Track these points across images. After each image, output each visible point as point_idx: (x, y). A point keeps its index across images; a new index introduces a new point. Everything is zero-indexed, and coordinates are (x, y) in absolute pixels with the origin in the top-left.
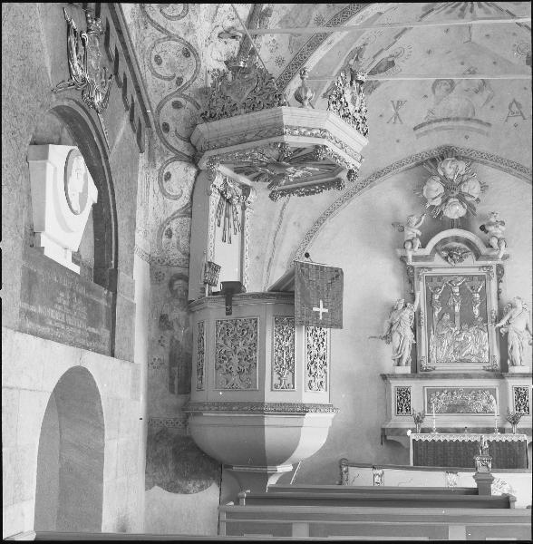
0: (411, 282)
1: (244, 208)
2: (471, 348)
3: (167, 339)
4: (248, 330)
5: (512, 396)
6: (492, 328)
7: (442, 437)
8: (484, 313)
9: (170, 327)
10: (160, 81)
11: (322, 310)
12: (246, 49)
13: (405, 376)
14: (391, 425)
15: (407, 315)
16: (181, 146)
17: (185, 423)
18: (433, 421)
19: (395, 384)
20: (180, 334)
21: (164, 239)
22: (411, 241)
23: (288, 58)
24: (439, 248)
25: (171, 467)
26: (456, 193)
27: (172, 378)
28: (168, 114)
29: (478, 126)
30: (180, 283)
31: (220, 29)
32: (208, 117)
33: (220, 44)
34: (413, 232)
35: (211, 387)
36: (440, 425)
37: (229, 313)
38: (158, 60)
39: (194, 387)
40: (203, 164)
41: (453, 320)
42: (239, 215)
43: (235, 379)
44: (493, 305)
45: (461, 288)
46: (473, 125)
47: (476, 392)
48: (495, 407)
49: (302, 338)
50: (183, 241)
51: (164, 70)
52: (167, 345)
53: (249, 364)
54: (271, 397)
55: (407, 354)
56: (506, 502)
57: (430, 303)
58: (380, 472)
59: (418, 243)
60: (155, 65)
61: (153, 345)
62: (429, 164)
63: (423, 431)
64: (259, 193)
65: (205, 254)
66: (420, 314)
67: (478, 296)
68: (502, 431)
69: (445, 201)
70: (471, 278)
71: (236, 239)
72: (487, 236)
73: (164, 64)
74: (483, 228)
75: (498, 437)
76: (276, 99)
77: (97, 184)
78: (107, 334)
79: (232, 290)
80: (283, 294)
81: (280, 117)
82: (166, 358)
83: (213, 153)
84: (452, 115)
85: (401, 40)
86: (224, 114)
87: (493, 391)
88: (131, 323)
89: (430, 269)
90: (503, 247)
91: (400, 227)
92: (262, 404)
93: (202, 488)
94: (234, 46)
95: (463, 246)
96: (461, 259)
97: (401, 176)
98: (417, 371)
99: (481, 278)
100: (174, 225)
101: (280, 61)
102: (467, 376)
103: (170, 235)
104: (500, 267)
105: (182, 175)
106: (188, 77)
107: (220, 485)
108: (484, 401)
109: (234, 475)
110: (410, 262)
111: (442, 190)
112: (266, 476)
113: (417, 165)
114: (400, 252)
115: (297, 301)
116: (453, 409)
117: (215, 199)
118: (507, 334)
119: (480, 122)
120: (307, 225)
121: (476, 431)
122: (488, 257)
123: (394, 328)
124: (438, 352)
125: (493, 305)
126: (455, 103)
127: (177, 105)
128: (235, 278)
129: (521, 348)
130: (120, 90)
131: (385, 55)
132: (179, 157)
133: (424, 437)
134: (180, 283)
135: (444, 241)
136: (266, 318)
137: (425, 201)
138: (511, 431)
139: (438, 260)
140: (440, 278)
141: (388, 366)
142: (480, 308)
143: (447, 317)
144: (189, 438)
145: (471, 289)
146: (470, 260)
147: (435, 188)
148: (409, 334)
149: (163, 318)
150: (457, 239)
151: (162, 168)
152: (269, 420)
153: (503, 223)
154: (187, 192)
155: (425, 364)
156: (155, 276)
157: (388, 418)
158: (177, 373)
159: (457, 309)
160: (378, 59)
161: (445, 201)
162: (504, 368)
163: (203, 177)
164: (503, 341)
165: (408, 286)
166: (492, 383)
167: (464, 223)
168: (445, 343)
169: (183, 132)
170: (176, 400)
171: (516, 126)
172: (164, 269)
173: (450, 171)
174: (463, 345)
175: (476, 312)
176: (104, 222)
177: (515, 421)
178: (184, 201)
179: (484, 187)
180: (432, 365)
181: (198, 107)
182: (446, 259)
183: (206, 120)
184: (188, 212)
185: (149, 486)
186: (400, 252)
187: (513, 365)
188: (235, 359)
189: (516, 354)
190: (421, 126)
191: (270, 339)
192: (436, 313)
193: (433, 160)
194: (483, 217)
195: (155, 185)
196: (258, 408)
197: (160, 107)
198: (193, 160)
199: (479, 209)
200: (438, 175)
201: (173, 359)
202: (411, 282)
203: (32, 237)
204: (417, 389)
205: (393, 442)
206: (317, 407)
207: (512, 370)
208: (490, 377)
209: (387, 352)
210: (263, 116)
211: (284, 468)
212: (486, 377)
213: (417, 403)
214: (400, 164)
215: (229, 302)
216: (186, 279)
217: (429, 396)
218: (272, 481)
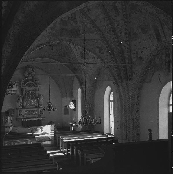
5: (40, 111)
13: (21, 109)
19: (19, 110)
41: (29, 98)
44: (37, 95)
49: (9, 118)
54: (6, 126)
57: (25, 94)
63: (24, 118)
68: (38, 118)
70: (32, 90)
74: (35, 81)
75: (37, 119)
87: (36, 111)
89: (25, 88)
91: (20, 81)
96: (31, 87)
98: (23, 107)
99: (35, 90)
104: (38, 88)
114: (20, 86)
116: (29, 114)
122: (36, 87)
124: (27, 103)
135: (28, 83)
138: (39, 118)
139: (27, 87)
141: (18, 106)
143: (28, 97)
146: (33, 87)
147: (27, 74)
148: (22, 101)
150: (31, 83)
157: (17, 116)
159: (30, 96)
164: (38, 102)
166: (37, 109)
167: (32, 80)
173: (29, 70)
174: (31, 102)
179: (36, 73)
182: (28, 87)
192: (27, 97)
196: (4, 127)
209: (17, 104)
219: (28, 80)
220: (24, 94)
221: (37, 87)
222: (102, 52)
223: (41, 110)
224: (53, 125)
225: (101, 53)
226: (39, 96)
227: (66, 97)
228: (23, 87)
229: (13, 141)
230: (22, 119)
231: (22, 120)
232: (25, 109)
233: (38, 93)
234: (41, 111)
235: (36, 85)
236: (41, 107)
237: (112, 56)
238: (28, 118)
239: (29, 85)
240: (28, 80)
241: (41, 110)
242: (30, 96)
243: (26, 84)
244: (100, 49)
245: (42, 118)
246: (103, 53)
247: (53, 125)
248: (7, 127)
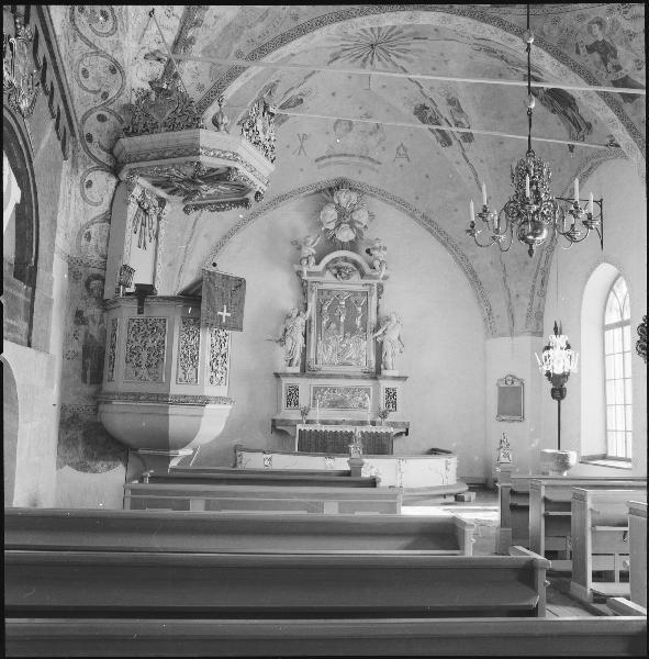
0: (305, 293)
1: (159, 219)
2: (352, 353)
3: (82, 333)
4: (156, 328)
5: (383, 394)
6: (371, 337)
7: (323, 428)
8: (364, 323)
9: (84, 323)
10: (86, 93)
11: (225, 314)
12: (170, 73)
13: (295, 375)
14: (278, 417)
15: (301, 321)
16: (103, 157)
17: (96, 410)
18: (318, 414)
19: (285, 381)
20: (94, 330)
21: (84, 241)
23: (208, 85)
24: (331, 265)
25: (80, 448)
26: (348, 220)
27: (84, 368)
28: (92, 126)
29: (370, 164)
30: (97, 285)
31: (146, 51)
32: (131, 132)
33: (146, 65)
34: (309, 250)
35: (121, 378)
36: (321, 417)
37: (140, 312)
38: (85, 72)
39: (106, 377)
40: (124, 176)
42: (154, 227)
43: (143, 372)
44: (373, 318)
45: (348, 301)
46: (367, 162)
47: (354, 391)
48: (369, 403)
49: (207, 338)
50: (102, 245)
51: (91, 84)
52: (81, 338)
53: (157, 360)
54: (176, 389)
55: (298, 357)
56: (373, 483)
57: (320, 312)
58: (269, 456)
59: (313, 260)
60: (82, 78)
61: (68, 338)
63: (308, 422)
64: (174, 206)
65: (121, 257)
66: (310, 322)
67: (360, 309)
68: (373, 424)
69: (338, 226)
70: (355, 293)
71: (151, 246)
72: (372, 258)
73: (91, 75)
74: (368, 251)
76: (194, 122)
77: (20, 185)
78: (26, 325)
79: (145, 292)
80: (191, 297)
81: (197, 139)
82: (80, 350)
83: (133, 166)
84: (349, 152)
85: (310, 81)
86: (146, 131)
87: (367, 391)
88: (48, 319)
92: (168, 396)
93: (109, 468)
94: (159, 68)
95: (351, 265)
96: (348, 277)
97: (302, 201)
98: (306, 370)
100: (93, 229)
101: (200, 88)
102: (348, 377)
103: (89, 237)
104: (380, 287)
105: (103, 183)
107: (126, 466)
108: (360, 399)
109: (138, 456)
110: (305, 277)
111: (336, 216)
112: (169, 459)
113: (319, 192)
114: (296, 267)
115: (204, 306)
116: (334, 404)
117: (133, 208)
119: (373, 160)
120: (216, 238)
121: (352, 423)
123: (288, 333)
124: (325, 355)
125: (373, 318)
126: (352, 142)
127: (101, 118)
128: (149, 282)
129: (393, 355)
130: (47, 99)
131: (295, 92)
132: (101, 167)
133: (308, 428)
134: (97, 285)
135: (334, 260)
136: (174, 318)
137: (321, 224)
139: (329, 276)
140: (329, 291)
141: (281, 366)
142: (361, 319)
144: (101, 424)
145: (355, 303)
146: (356, 277)
148: (301, 340)
149: (79, 314)
151: (83, 179)
152: (172, 410)
153: (385, 249)
154: (107, 199)
155: (313, 365)
156: (74, 275)
157: (278, 411)
158: (91, 363)
160: (289, 96)
161: (338, 226)
162: (378, 371)
163: (123, 187)
164: (379, 348)
165: (302, 297)
166: (368, 383)
168: (331, 349)
169: (105, 143)
170: (89, 389)
171: (401, 166)
172: (81, 269)
174: (345, 351)
175: (358, 322)
177: (384, 415)
178: (104, 207)
179: (372, 216)
180: (318, 366)
181: (121, 121)
182: (336, 275)
183: (128, 135)
184: (108, 218)
185: (59, 466)
186: (296, 267)
188: (145, 354)
189: (389, 360)
190: (323, 158)
191: (176, 340)
192: (324, 322)
193: (330, 189)
194: (371, 243)
195: (76, 190)
196: (163, 399)
197: (84, 120)
198: (115, 170)
199: (366, 235)
200: (333, 202)
201: (86, 349)
202: (305, 293)
204: (305, 386)
206: (219, 400)
207: (384, 372)
208: (365, 378)
210: (183, 136)
211: (183, 452)
212: (364, 378)
213: (304, 400)
214: (300, 190)
215: (141, 304)
216: (103, 280)
217: (315, 392)
218: (174, 463)
219: (332, 244)
220: (312, 306)
221: (375, 282)
223: (387, 390)
224: (453, 461)
227: (512, 334)
229: (197, 494)
230: (300, 422)
231: (299, 427)
232: (314, 376)
234: (391, 395)
238: (324, 423)
239: (339, 272)
240: (332, 244)
241: (387, 390)
242: (342, 320)
247: (453, 461)
248: (183, 401)
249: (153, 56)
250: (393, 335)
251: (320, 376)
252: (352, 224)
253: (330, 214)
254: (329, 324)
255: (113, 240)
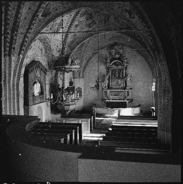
12: (63, 53)
15: (107, 77)
18: (111, 97)
22: (108, 63)
36: (112, 99)
38: (49, 57)
44: (124, 75)
57: (112, 74)
62: (111, 47)
63: (109, 99)
68: (124, 99)
70: (120, 69)
75: (123, 101)
87: (123, 92)
90: (126, 64)
98: (109, 88)
106: (53, 59)
118: (126, 81)
122: (123, 66)
124: (113, 83)
125: (124, 75)
132: (54, 69)
134: (55, 88)
139: (114, 66)
142: (122, 76)
148: (107, 81)
150: (117, 62)
166: (123, 90)
167: (119, 59)
176: (41, 87)
187: (127, 87)
193: (113, 45)
198: (55, 69)
203: (34, 95)
205: (104, 101)
219: (115, 59)
222: (132, 16)
223: (127, 91)
225: (131, 18)
226: (126, 75)
228: (109, 66)
230: (107, 99)
232: (110, 89)
233: (126, 74)
234: (128, 92)
235: (123, 64)
236: (127, 88)
237: (142, 20)
239: (115, 64)
240: (115, 59)
241: (127, 91)
243: (113, 62)
244: (130, 14)
245: (128, 100)
246: (134, 18)
248: (66, 105)
249: (59, 51)
250: (129, 79)
251: (112, 89)
252: (119, 53)
253: (113, 51)
254: (114, 77)
255: (56, 80)
